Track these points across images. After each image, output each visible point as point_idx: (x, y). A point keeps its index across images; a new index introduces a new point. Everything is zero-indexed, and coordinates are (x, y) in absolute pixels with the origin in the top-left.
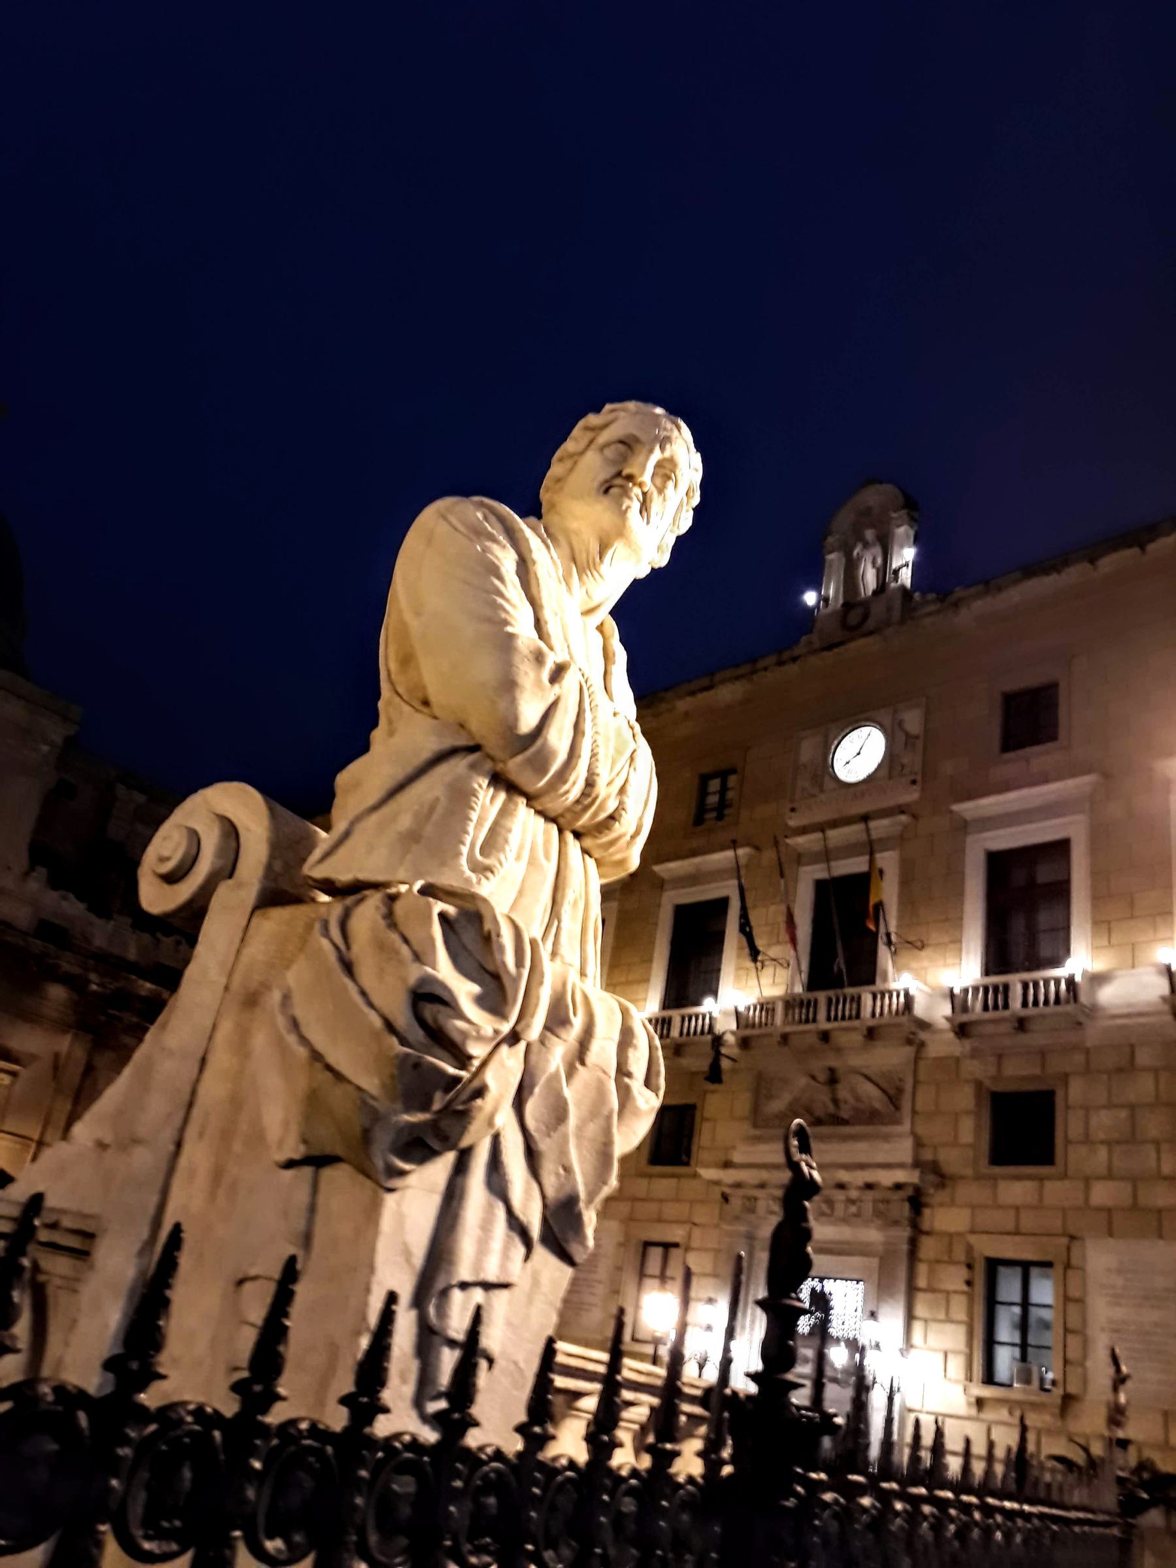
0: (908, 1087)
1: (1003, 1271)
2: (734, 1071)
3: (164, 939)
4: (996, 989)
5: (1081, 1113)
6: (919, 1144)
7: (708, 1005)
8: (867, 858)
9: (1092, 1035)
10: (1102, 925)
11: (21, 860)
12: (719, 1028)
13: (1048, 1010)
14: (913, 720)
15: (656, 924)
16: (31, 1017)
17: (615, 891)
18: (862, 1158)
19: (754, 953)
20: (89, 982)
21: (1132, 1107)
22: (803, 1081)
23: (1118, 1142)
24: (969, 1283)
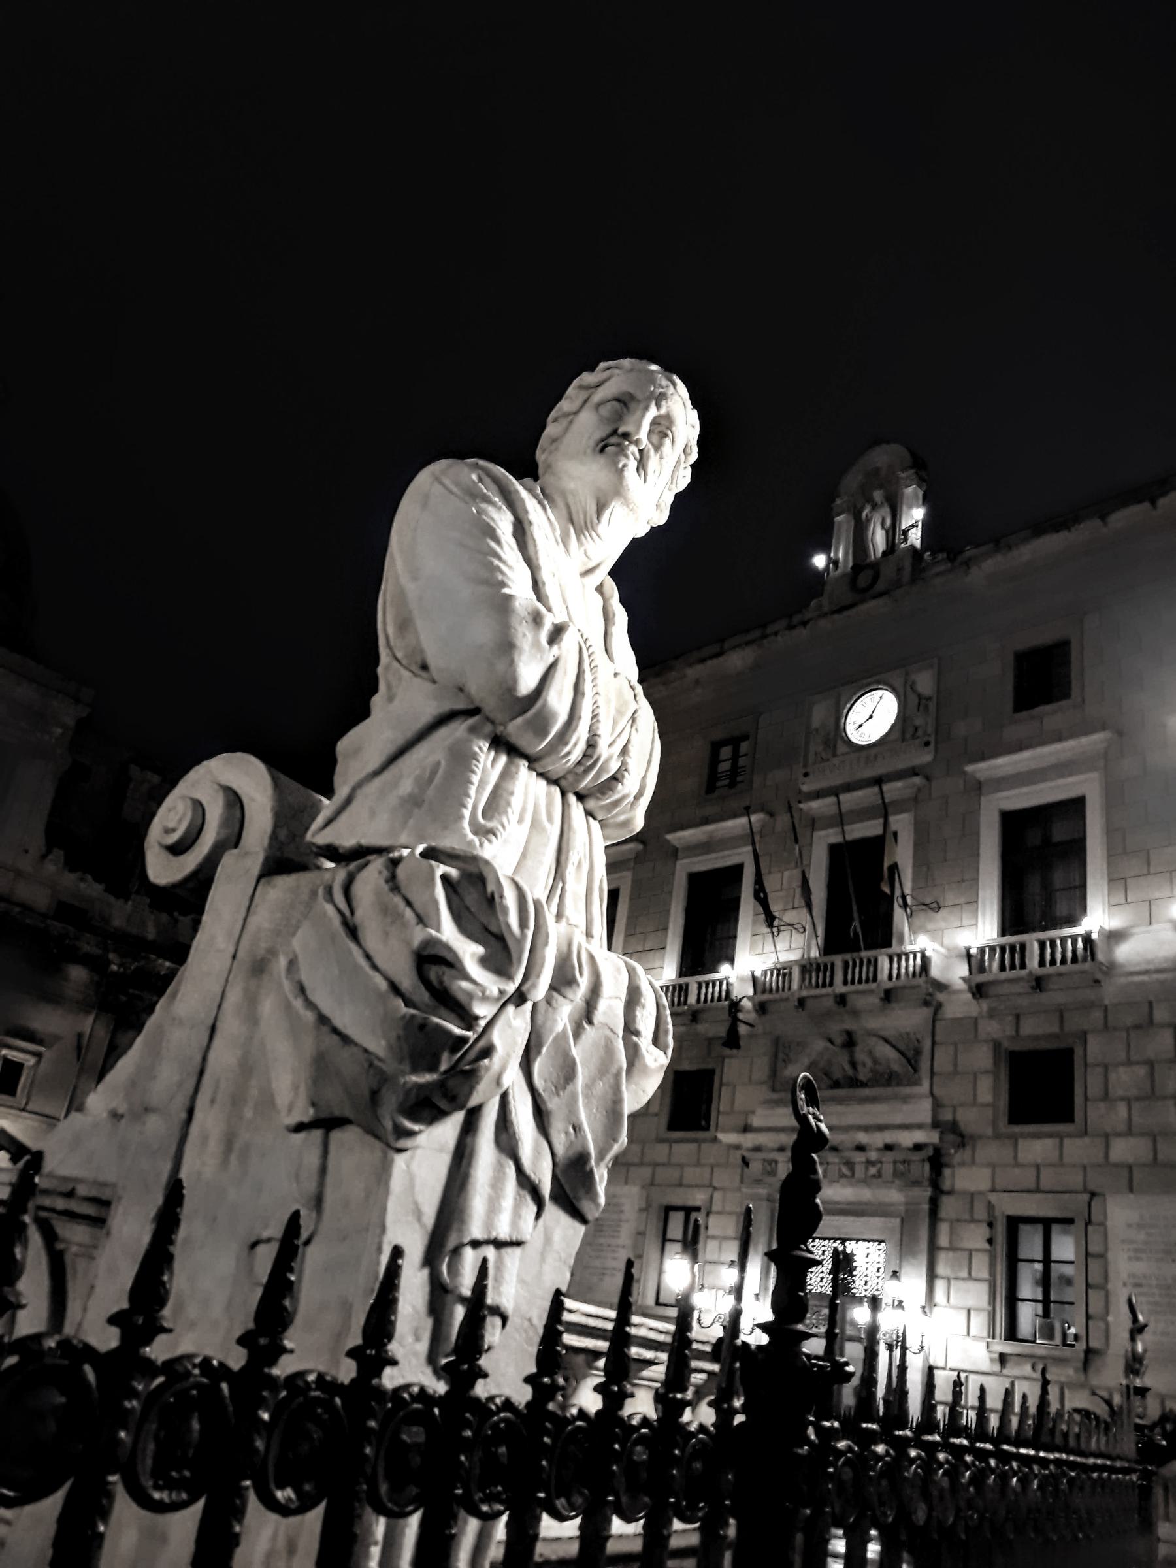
0: (927, 1045)
1: (1025, 1230)
2: (751, 1036)
3: (181, 918)
4: (1012, 948)
5: (1100, 1070)
6: (937, 1105)
7: (725, 970)
8: (881, 820)
9: (1110, 992)
10: (1118, 881)
11: (37, 842)
12: (736, 993)
13: (1063, 969)
14: (925, 682)
15: (671, 893)
16: (54, 999)
17: (629, 860)
18: (881, 1120)
19: (770, 919)
20: (109, 963)
21: (1151, 1064)
22: (820, 1045)
23: (1138, 1099)
24: (990, 1241)
